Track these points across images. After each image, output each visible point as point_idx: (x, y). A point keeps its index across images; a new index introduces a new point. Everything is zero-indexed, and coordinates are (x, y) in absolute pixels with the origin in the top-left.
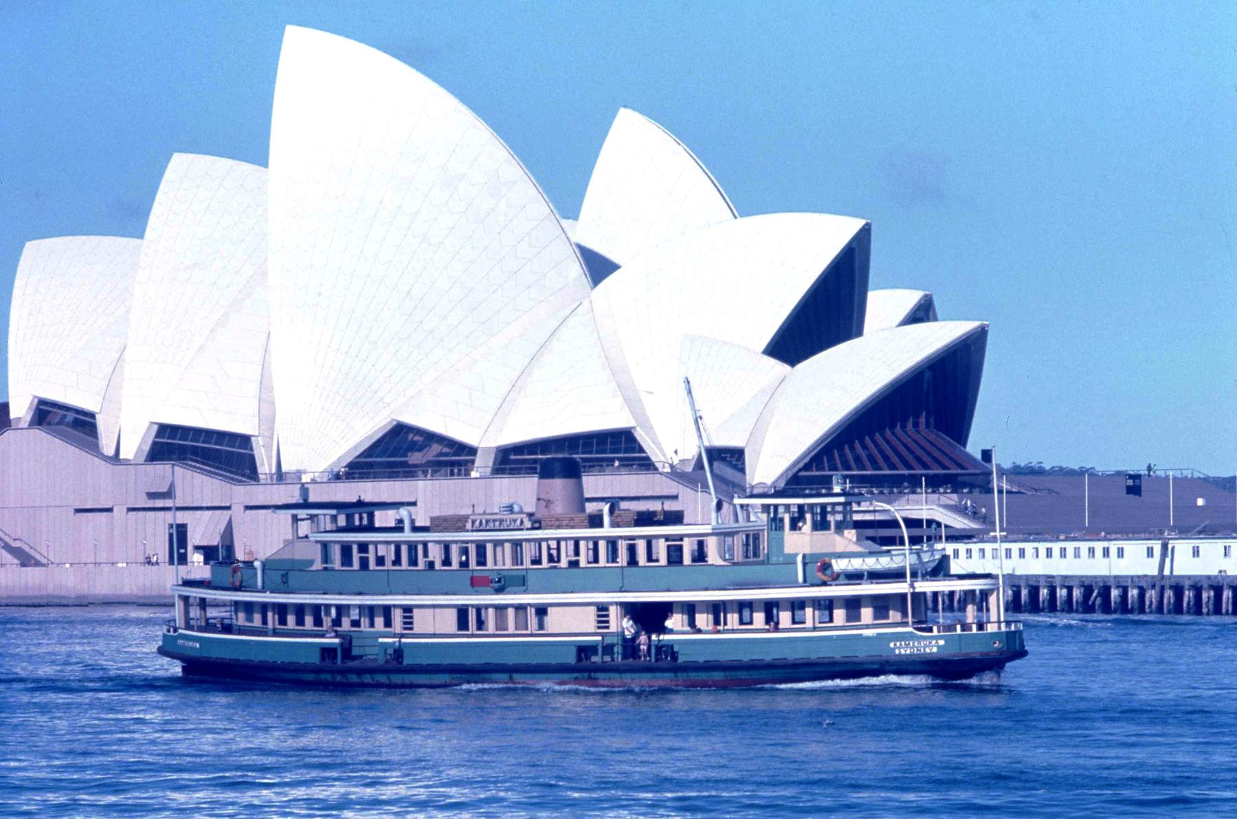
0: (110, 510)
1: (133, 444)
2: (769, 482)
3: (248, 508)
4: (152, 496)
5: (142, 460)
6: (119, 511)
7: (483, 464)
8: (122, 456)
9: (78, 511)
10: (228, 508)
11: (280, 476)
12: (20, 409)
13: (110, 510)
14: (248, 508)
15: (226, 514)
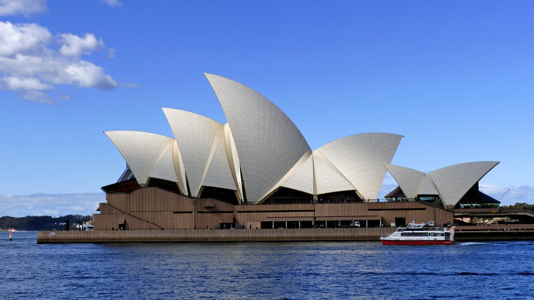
0: (191, 212)
1: (195, 193)
2: (454, 205)
3: (239, 212)
4: (207, 208)
5: (199, 197)
6: (194, 212)
7: (316, 198)
8: (192, 196)
9: (174, 213)
10: (232, 212)
11: (246, 202)
12: (142, 180)
13: (191, 212)
14: (239, 212)
15: (232, 214)
